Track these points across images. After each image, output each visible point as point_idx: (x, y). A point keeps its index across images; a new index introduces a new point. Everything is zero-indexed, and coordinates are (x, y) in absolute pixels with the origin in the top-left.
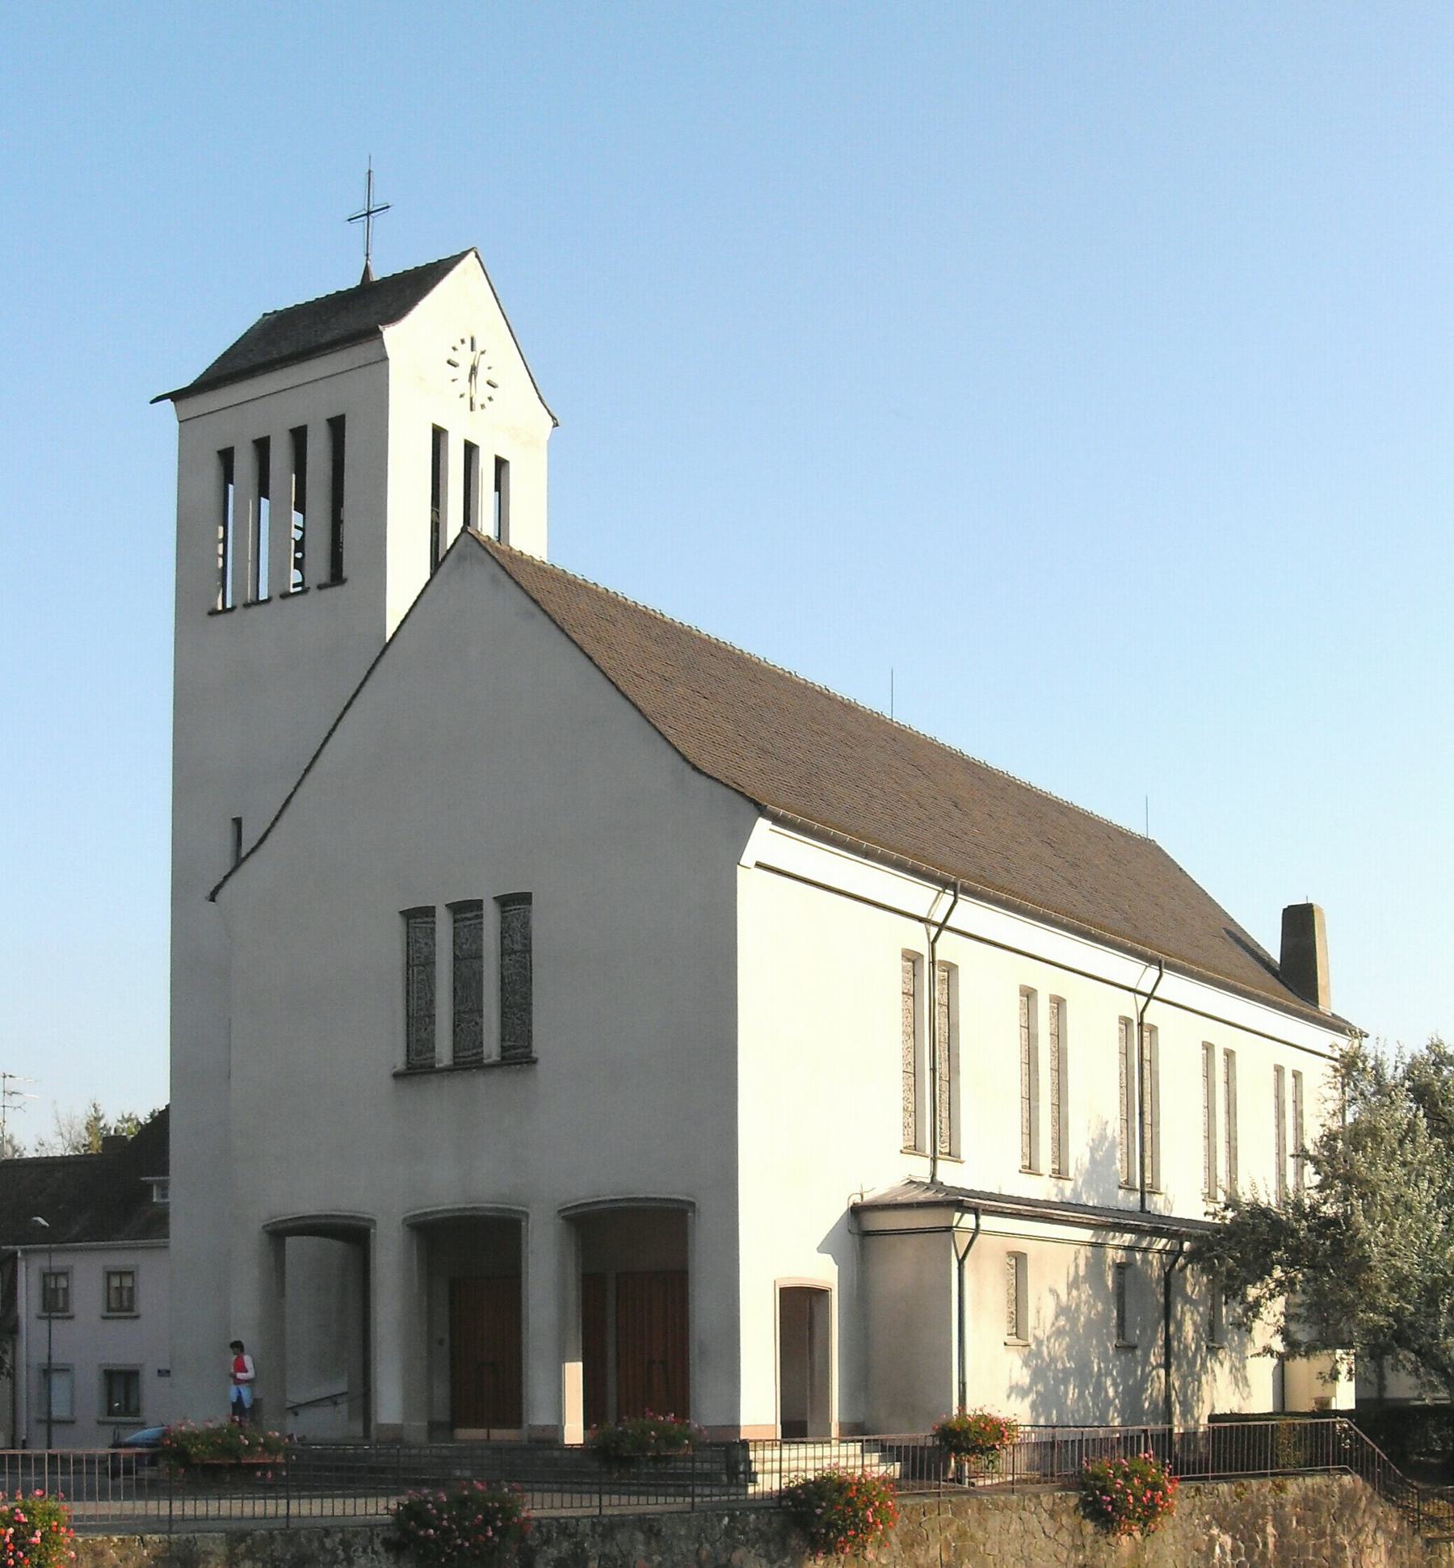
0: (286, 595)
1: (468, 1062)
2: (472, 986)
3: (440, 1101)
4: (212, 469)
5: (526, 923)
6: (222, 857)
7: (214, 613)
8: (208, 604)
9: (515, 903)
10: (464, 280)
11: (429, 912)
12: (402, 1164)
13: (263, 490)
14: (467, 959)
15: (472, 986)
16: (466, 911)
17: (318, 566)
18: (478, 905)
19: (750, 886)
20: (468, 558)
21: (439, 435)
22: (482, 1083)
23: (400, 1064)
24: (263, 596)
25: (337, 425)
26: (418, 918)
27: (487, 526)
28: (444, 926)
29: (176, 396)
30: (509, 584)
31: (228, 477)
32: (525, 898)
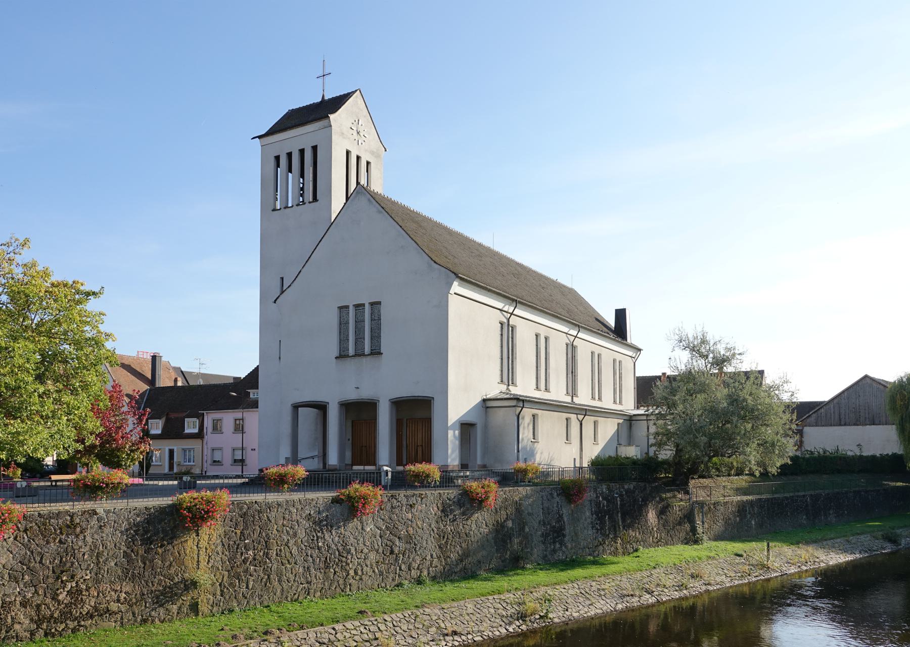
0: (298, 205)
1: (359, 354)
2: (360, 332)
3: (350, 365)
4: (272, 162)
5: (379, 311)
6: (277, 290)
7: (274, 210)
8: (271, 208)
9: (375, 305)
10: (356, 97)
11: (347, 307)
12: (339, 385)
13: (290, 171)
14: (359, 322)
15: (360, 332)
16: (359, 307)
17: (309, 195)
18: (364, 305)
19: (453, 300)
20: (359, 194)
21: (348, 153)
22: (364, 360)
23: (336, 354)
24: (290, 205)
25: (315, 148)
26: (343, 309)
27: (363, 181)
28: (352, 310)
29: (260, 137)
30: (374, 202)
31: (278, 166)
32: (379, 303)
